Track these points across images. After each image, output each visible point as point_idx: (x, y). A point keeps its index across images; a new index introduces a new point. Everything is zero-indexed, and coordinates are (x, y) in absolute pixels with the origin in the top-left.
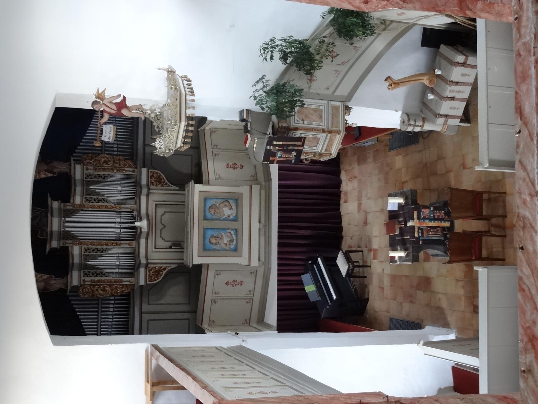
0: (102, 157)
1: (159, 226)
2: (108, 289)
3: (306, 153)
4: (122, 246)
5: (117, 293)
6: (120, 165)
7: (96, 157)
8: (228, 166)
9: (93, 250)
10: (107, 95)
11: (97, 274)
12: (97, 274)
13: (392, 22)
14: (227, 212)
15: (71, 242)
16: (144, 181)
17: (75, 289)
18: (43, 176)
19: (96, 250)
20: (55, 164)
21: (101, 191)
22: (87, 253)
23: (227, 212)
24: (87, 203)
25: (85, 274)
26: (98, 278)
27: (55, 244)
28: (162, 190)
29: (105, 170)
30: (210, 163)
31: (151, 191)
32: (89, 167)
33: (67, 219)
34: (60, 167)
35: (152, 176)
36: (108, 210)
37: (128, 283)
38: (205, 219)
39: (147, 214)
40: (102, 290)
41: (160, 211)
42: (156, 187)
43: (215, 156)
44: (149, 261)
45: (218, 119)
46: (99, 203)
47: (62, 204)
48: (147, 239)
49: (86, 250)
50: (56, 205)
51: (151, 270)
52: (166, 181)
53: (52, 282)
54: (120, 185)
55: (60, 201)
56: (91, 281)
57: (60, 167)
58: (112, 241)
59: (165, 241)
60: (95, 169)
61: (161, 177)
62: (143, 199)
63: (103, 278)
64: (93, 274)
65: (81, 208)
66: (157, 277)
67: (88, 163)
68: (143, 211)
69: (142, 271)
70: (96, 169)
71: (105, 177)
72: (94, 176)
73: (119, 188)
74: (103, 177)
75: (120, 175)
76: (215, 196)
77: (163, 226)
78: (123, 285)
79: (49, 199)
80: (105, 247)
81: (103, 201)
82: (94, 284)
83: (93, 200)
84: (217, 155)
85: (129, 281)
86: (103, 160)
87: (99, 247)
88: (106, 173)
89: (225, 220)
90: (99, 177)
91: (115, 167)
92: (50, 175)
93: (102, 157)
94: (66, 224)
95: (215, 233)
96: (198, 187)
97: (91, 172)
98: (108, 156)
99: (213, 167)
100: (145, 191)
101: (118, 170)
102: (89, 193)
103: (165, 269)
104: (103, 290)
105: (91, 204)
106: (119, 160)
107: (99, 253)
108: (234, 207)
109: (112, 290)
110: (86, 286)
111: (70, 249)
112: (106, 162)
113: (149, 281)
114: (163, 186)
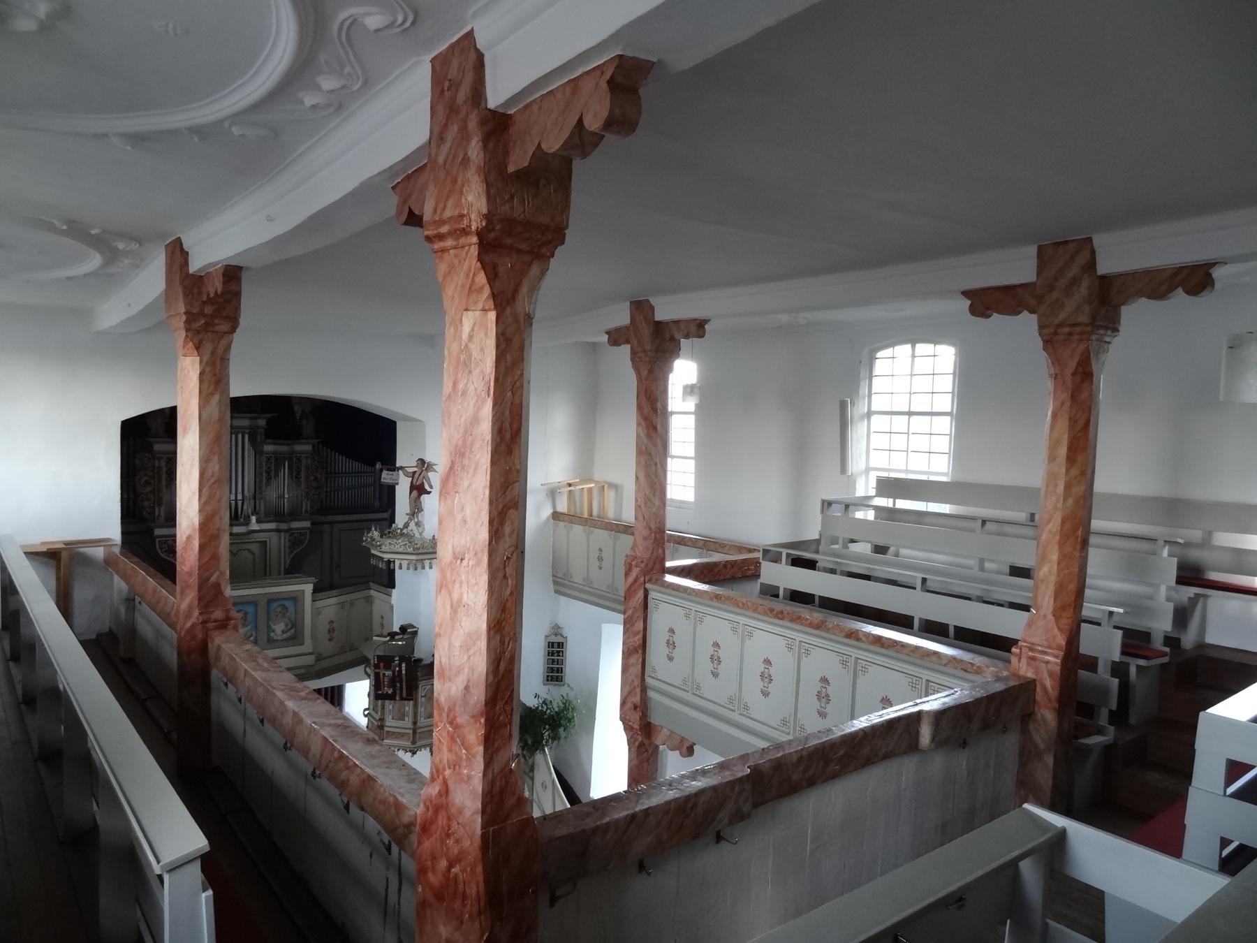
2: (148, 489)
3: (383, 708)
8: (332, 622)
10: (431, 475)
13: (532, 779)
14: (279, 628)
16: (295, 525)
17: (149, 448)
18: (296, 408)
23: (279, 628)
30: (333, 601)
34: (308, 428)
38: (270, 601)
41: (255, 548)
43: (342, 605)
45: (393, 602)
50: (262, 422)
56: (160, 468)
57: (308, 428)
60: (307, 467)
63: (164, 483)
65: (258, 452)
71: (298, 478)
76: (299, 610)
79: (269, 415)
84: (343, 607)
88: (303, 479)
89: (269, 627)
92: (298, 416)
95: (250, 617)
96: (308, 588)
97: (304, 462)
99: (330, 604)
100: (284, 526)
104: (147, 483)
108: (285, 636)
112: (316, 478)
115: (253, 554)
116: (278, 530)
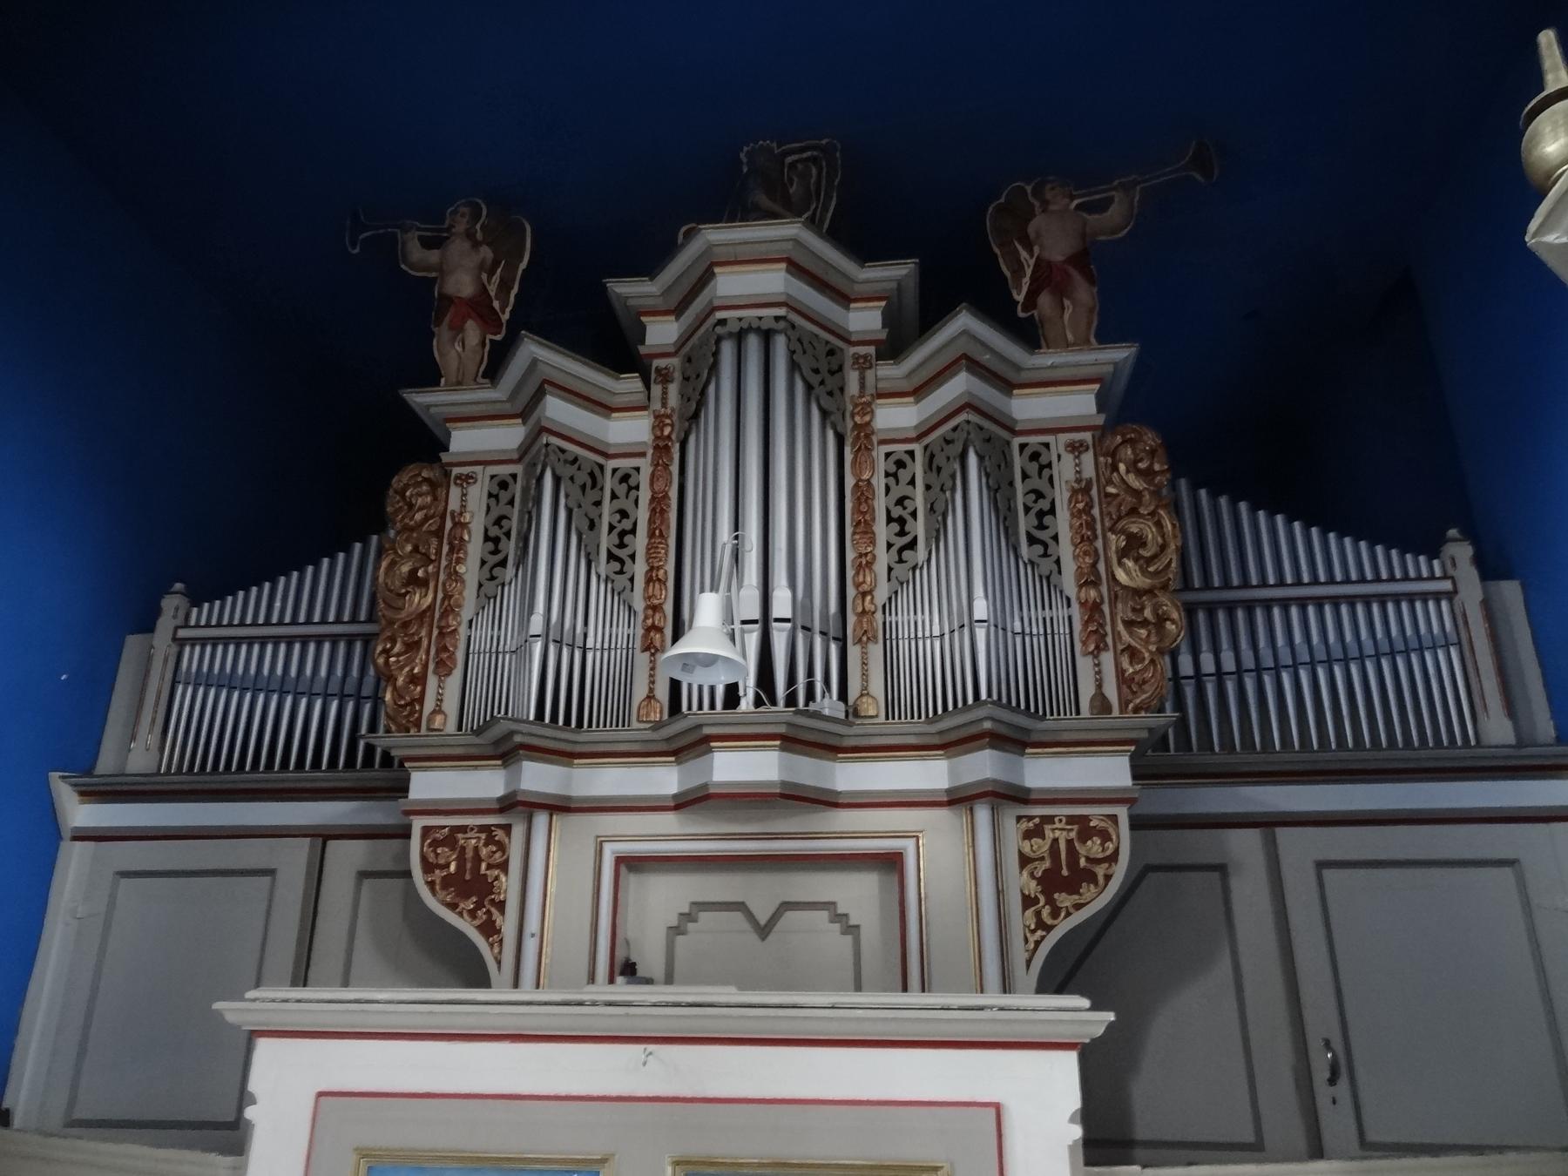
0: (1159, 524)
1: (762, 891)
2: (419, 600)
4: (642, 659)
5: (386, 652)
6: (1129, 624)
7: (1156, 494)
9: (624, 514)
11: (496, 540)
12: (496, 540)
15: (673, 400)
16: (1043, 772)
19: (627, 524)
20: (1084, 293)
21: (955, 522)
22: (609, 483)
24: (882, 466)
25: (503, 485)
26: (475, 547)
27: (662, 333)
28: (999, 893)
29: (1085, 539)
31: (983, 814)
32: (1088, 458)
33: (780, 345)
35: (1085, 828)
36: (850, 571)
37: (429, 705)
39: (829, 801)
40: (414, 572)
42: (1012, 861)
44: (541, 820)
46: (885, 523)
47: (871, 350)
48: (683, 803)
49: (625, 478)
50: (866, 320)
51: (490, 840)
52: (1063, 927)
53: (472, 331)
54: (999, 625)
55: (883, 336)
58: (669, 608)
59: (676, 931)
60: (1081, 490)
61: (1088, 890)
62: (932, 774)
63: (470, 570)
64: (498, 522)
65: (851, 437)
66: (447, 882)
67: (1113, 454)
68: (850, 776)
69: (487, 783)
70: (1086, 490)
71: (1042, 542)
72: (1041, 485)
73: (981, 609)
74: (1044, 535)
75: (1063, 629)
77: (763, 919)
78: (419, 680)
80: (640, 569)
81: (900, 542)
82: (449, 524)
83: (897, 492)
85: (438, 710)
86: (1150, 533)
87: (640, 542)
88: (1066, 550)
90: (1041, 514)
91: (1114, 599)
93: (1159, 524)
94: (753, 344)
97: (1064, 470)
98: (1171, 555)
100: (983, 765)
101: (1093, 610)
102: (937, 461)
103: (490, 929)
104: (413, 580)
105: (879, 482)
106: (1161, 620)
107: (606, 541)
109: (406, 625)
110: (441, 492)
111: (630, 385)
112: (1134, 544)
113: (426, 831)
114: (1028, 901)
115: (852, 930)
116: (959, 799)
